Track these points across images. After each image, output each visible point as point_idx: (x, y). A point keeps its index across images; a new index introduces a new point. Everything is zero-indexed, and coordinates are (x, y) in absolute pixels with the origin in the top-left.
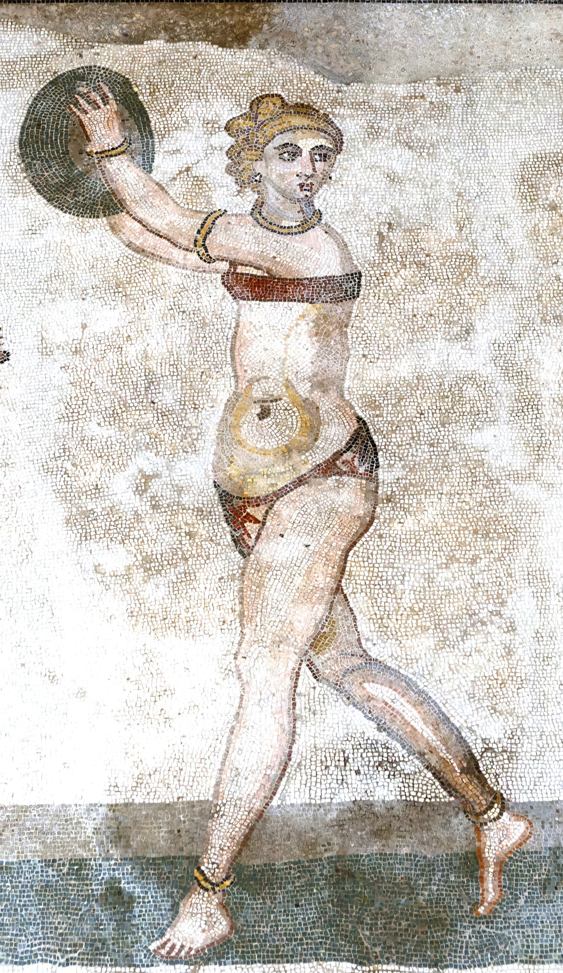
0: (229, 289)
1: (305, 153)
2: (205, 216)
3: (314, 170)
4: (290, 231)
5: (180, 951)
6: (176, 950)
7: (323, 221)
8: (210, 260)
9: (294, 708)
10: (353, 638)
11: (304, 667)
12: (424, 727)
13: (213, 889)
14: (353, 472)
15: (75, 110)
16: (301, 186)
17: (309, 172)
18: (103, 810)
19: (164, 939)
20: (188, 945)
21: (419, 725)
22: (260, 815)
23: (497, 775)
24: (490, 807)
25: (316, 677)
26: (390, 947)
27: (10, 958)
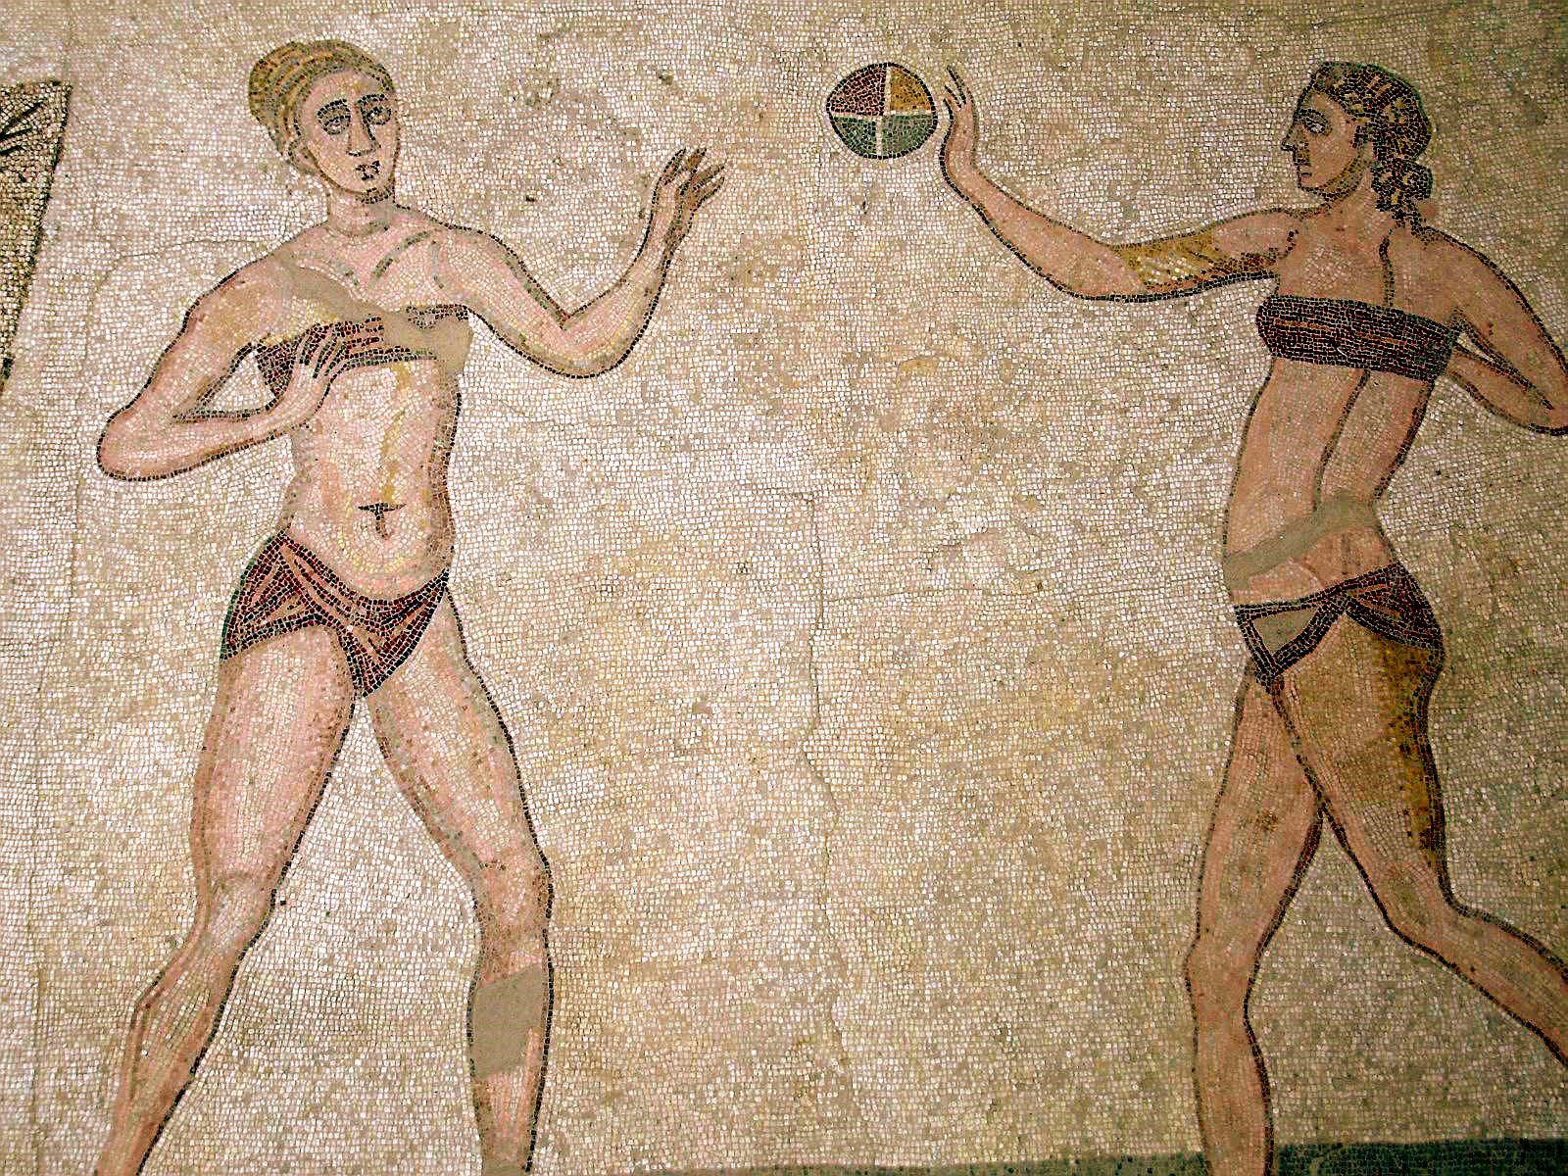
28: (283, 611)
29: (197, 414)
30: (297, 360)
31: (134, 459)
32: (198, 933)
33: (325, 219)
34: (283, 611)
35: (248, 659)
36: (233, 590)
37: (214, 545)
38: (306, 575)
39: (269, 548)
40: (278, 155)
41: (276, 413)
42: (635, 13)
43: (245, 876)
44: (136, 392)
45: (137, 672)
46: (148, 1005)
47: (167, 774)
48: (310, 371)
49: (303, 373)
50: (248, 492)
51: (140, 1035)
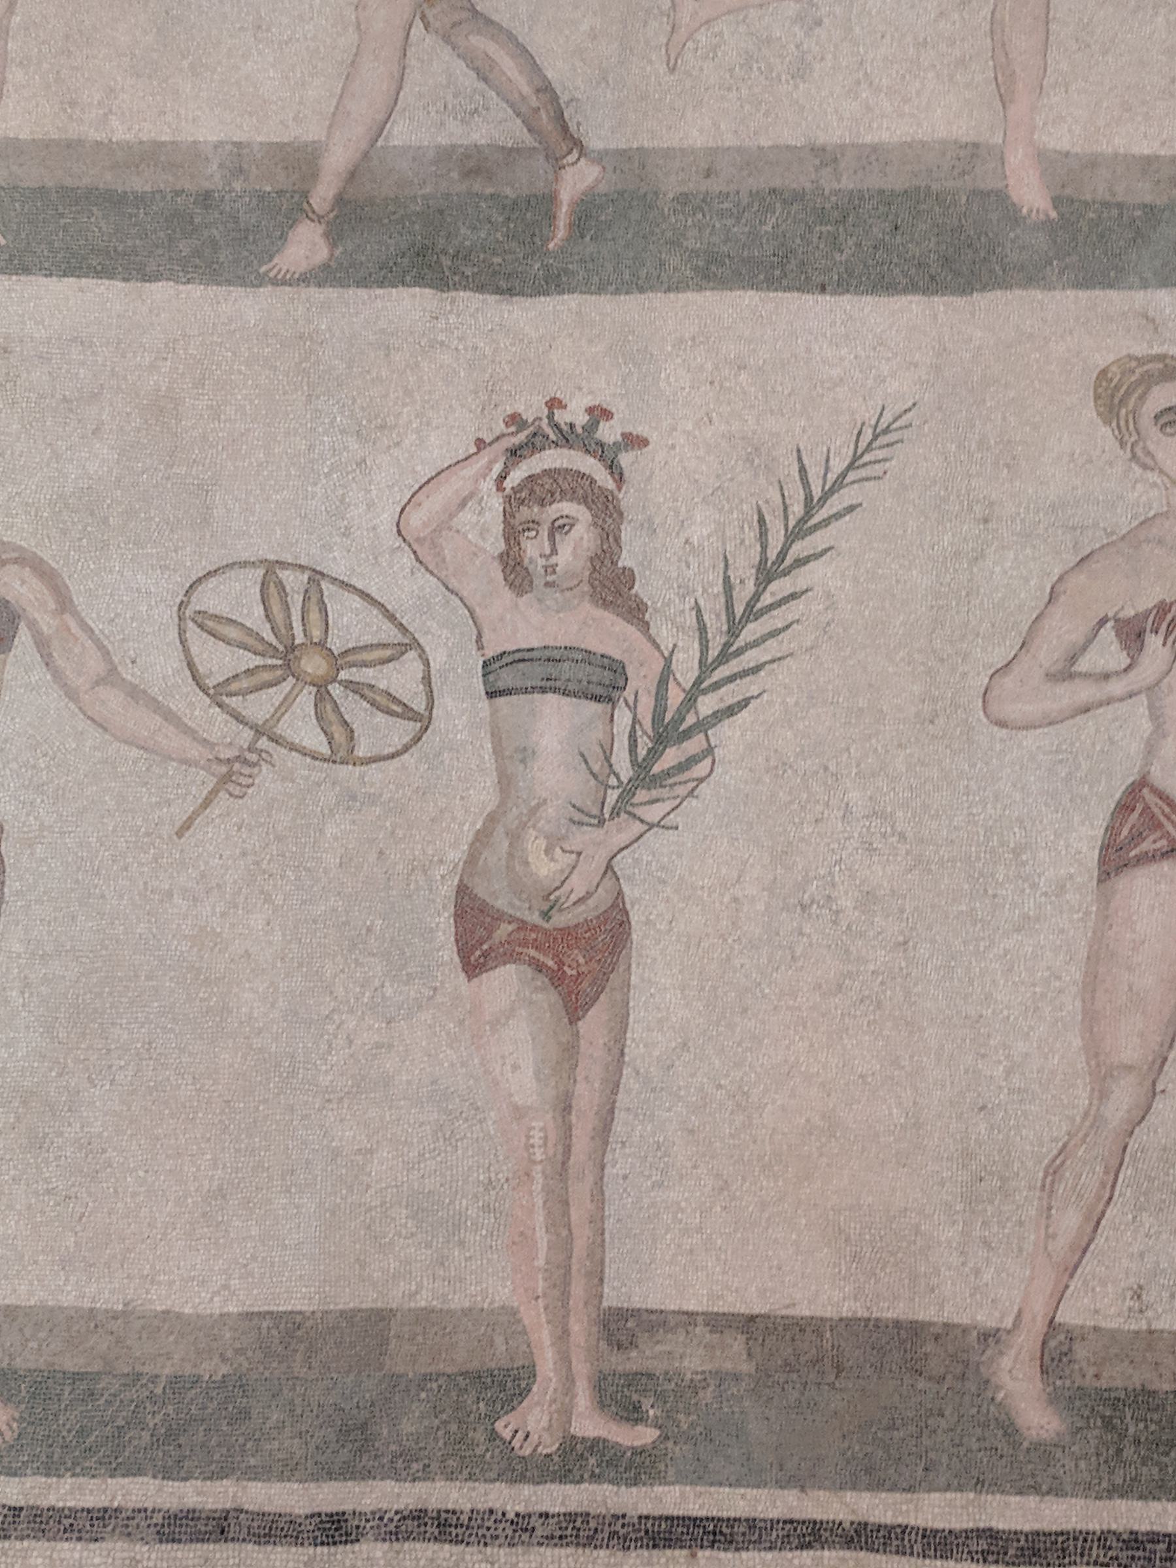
18: (229, 147)
20: (292, 269)
22: (366, 155)
23: (579, 124)
24: (570, 152)
28: (1146, 846)
29: (1065, 673)
30: (1148, 630)
31: (1013, 710)
32: (1092, 1113)
33: (1165, 509)
34: (1146, 846)
35: (1122, 883)
36: (1105, 824)
37: (1086, 786)
38: (1166, 816)
39: (1133, 791)
40: (1122, 453)
41: (1132, 674)
43: (1129, 1068)
44: (1013, 653)
45: (1028, 891)
46: (1054, 1171)
47: (1059, 978)
48: (1159, 639)
49: (1154, 642)
50: (1111, 741)
51: (1050, 1197)
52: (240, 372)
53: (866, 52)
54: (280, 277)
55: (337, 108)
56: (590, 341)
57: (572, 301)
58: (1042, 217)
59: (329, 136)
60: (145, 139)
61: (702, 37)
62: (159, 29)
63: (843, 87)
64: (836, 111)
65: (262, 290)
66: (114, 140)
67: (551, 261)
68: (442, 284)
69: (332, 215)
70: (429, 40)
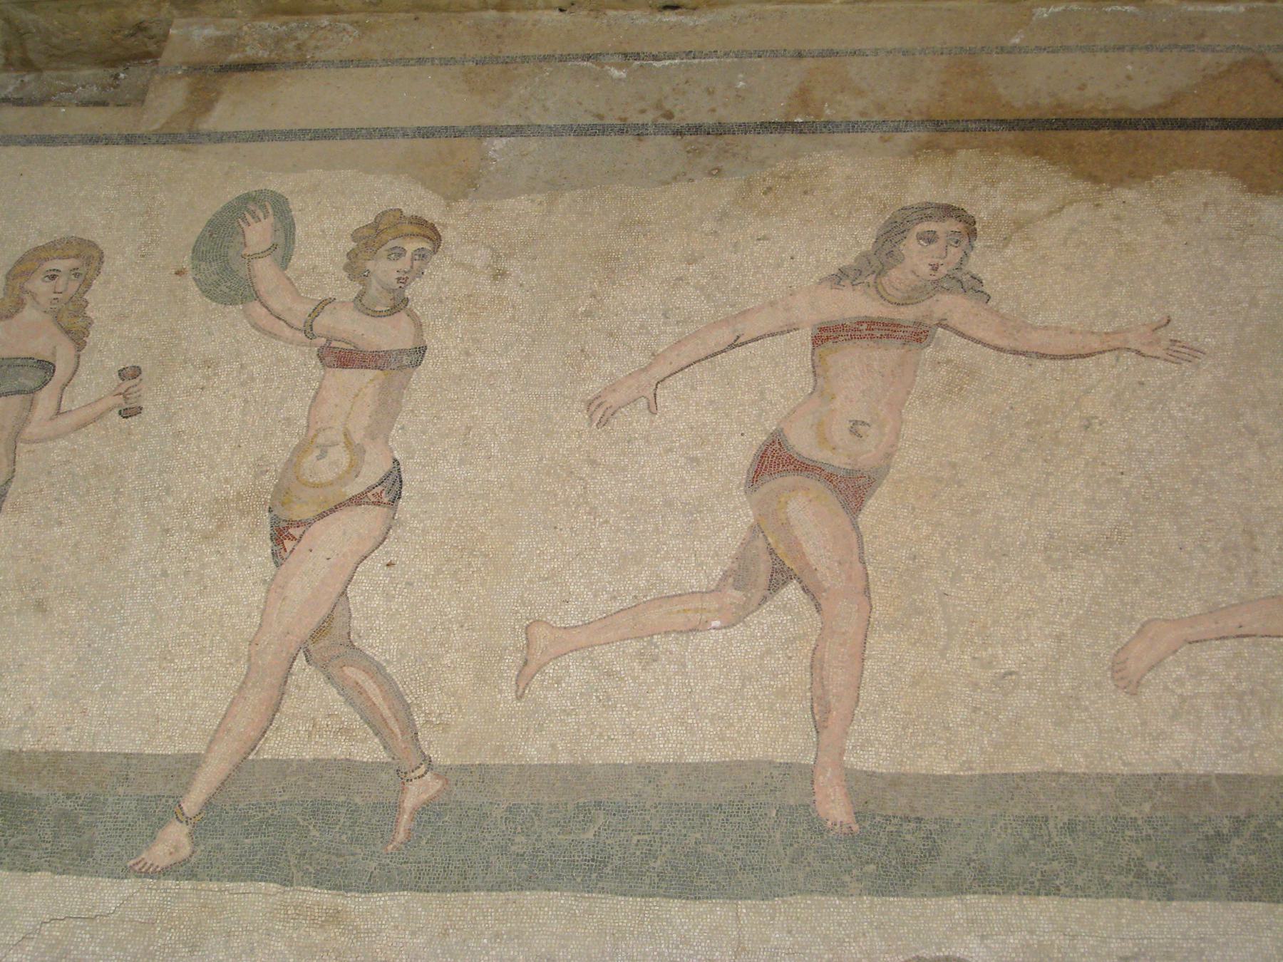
0: (321, 359)
1: (409, 254)
2: (317, 303)
3: (412, 267)
4: (381, 314)
5: (150, 868)
6: (146, 867)
7: (408, 307)
8: (314, 336)
9: (285, 685)
10: (344, 633)
11: (301, 655)
12: (382, 702)
13: (187, 821)
14: (378, 503)
15: (241, 223)
16: (399, 279)
17: (407, 268)
18: (119, 758)
19: (138, 860)
20: (157, 864)
21: (378, 700)
22: (237, 767)
25: (308, 661)
26: (311, 873)
27: (23, 866)
42: (1199, 941)
52: (94, 953)
53: (696, 684)
54: (143, 870)
55: (219, 725)
56: (413, 933)
57: (404, 897)
58: (845, 830)
59: (209, 749)
60: (50, 750)
61: (549, 670)
62: (79, 659)
63: (672, 714)
64: (664, 734)
65: (126, 881)
66: (24, 750)
67: (388, 861)
68: (286, 881)
69: (198, 818)
70: (310, 670)
